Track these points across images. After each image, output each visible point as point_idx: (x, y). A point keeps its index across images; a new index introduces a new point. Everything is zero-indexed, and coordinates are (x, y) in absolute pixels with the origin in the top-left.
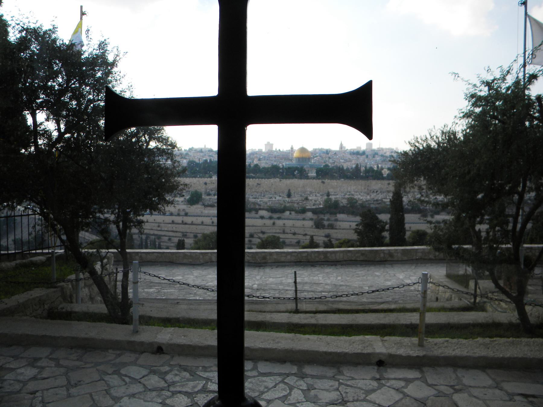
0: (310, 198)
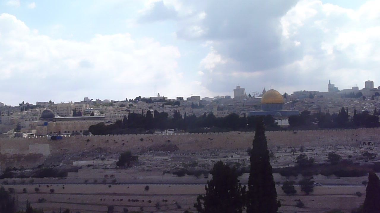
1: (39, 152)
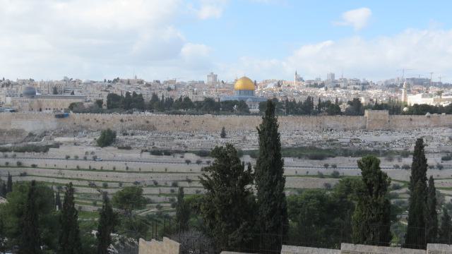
0: (248, 138)
1: (21, 127)
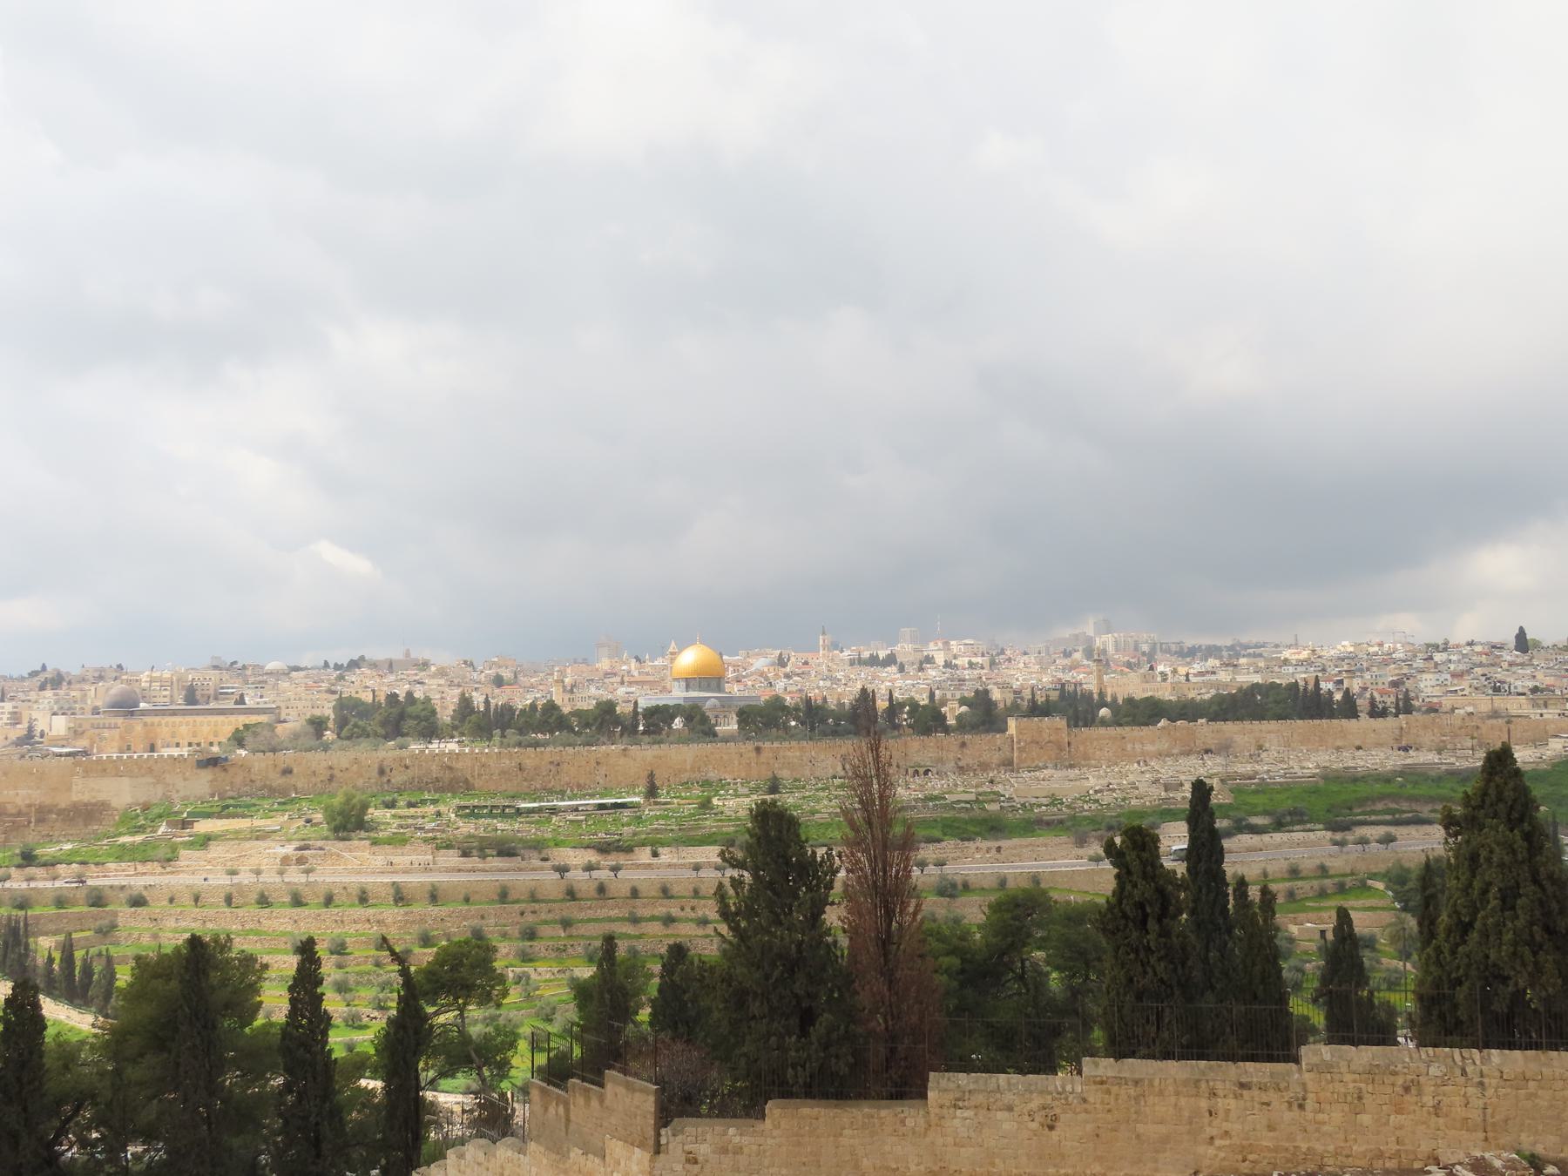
1: (102, 797)
